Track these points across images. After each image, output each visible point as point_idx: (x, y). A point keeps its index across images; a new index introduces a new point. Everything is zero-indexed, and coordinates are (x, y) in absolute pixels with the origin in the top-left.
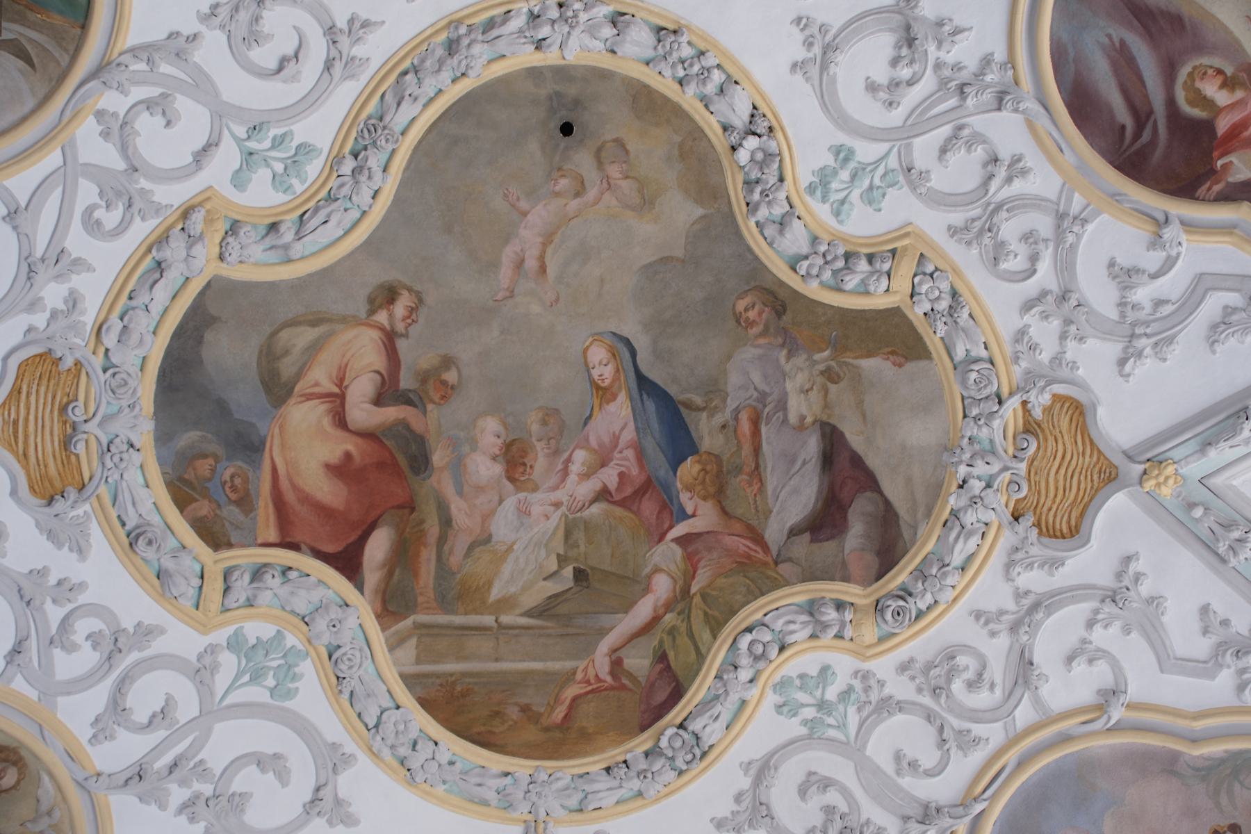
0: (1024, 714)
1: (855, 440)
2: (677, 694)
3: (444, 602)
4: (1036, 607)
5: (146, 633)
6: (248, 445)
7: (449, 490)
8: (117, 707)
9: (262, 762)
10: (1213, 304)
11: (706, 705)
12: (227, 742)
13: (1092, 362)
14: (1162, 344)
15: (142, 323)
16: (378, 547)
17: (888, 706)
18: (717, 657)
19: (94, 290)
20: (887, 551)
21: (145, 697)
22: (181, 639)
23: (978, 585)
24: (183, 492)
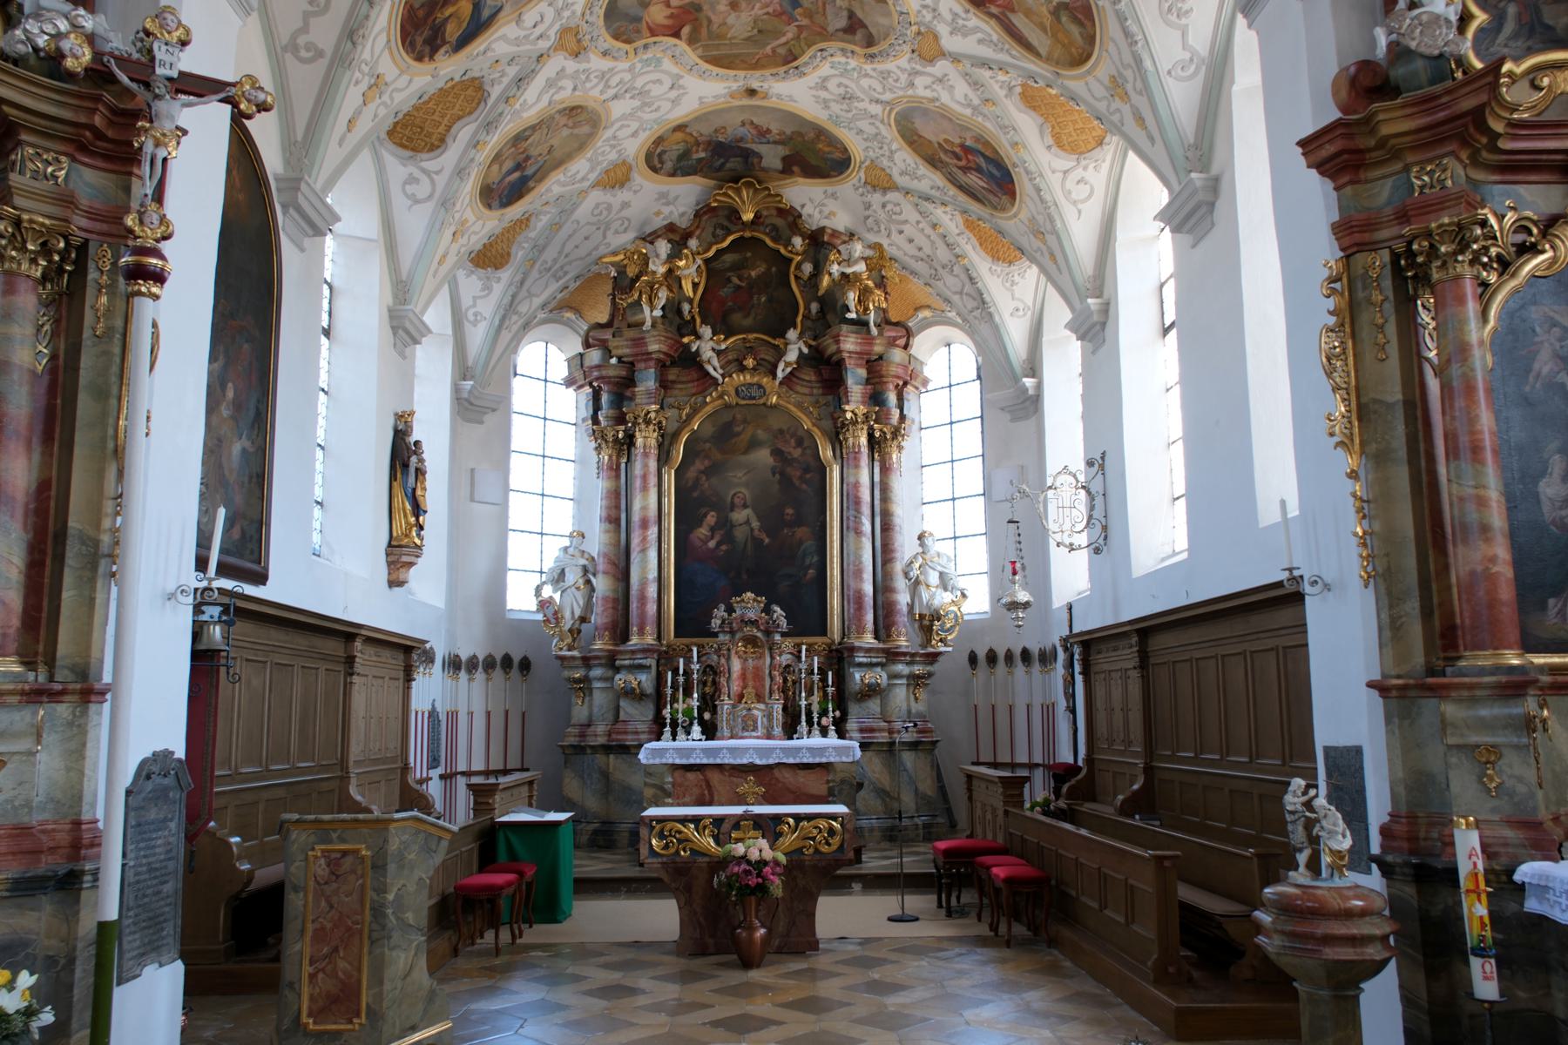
0: (910, 92)
1: (859, 14)
2: (795, 59)
3: (710, 38)
4: (918, 73)
5: (611, 70)
6: (638, 19)
7: (710, 13)
8: (607, 86)
9: (654, 82)
10: (979, 35)
11: (806, 64)
12: (639, 83)
13: (943, 30)
14: (965, 35)
15: (596, 9)
16: (686, 31)
17: (867, 75)
18: (810, 53)
19: (578, 8)
20: (870, 42)
21: (613, 82)
22: (623, 65)
23: (900, 63)
24: (616, 37)
